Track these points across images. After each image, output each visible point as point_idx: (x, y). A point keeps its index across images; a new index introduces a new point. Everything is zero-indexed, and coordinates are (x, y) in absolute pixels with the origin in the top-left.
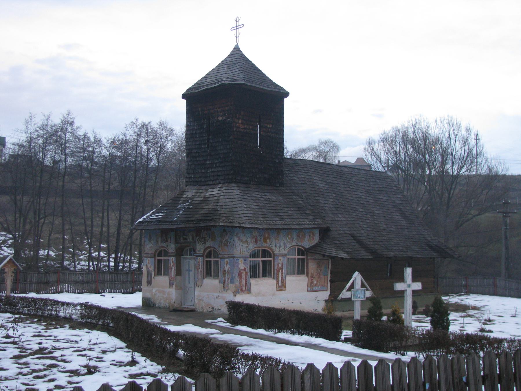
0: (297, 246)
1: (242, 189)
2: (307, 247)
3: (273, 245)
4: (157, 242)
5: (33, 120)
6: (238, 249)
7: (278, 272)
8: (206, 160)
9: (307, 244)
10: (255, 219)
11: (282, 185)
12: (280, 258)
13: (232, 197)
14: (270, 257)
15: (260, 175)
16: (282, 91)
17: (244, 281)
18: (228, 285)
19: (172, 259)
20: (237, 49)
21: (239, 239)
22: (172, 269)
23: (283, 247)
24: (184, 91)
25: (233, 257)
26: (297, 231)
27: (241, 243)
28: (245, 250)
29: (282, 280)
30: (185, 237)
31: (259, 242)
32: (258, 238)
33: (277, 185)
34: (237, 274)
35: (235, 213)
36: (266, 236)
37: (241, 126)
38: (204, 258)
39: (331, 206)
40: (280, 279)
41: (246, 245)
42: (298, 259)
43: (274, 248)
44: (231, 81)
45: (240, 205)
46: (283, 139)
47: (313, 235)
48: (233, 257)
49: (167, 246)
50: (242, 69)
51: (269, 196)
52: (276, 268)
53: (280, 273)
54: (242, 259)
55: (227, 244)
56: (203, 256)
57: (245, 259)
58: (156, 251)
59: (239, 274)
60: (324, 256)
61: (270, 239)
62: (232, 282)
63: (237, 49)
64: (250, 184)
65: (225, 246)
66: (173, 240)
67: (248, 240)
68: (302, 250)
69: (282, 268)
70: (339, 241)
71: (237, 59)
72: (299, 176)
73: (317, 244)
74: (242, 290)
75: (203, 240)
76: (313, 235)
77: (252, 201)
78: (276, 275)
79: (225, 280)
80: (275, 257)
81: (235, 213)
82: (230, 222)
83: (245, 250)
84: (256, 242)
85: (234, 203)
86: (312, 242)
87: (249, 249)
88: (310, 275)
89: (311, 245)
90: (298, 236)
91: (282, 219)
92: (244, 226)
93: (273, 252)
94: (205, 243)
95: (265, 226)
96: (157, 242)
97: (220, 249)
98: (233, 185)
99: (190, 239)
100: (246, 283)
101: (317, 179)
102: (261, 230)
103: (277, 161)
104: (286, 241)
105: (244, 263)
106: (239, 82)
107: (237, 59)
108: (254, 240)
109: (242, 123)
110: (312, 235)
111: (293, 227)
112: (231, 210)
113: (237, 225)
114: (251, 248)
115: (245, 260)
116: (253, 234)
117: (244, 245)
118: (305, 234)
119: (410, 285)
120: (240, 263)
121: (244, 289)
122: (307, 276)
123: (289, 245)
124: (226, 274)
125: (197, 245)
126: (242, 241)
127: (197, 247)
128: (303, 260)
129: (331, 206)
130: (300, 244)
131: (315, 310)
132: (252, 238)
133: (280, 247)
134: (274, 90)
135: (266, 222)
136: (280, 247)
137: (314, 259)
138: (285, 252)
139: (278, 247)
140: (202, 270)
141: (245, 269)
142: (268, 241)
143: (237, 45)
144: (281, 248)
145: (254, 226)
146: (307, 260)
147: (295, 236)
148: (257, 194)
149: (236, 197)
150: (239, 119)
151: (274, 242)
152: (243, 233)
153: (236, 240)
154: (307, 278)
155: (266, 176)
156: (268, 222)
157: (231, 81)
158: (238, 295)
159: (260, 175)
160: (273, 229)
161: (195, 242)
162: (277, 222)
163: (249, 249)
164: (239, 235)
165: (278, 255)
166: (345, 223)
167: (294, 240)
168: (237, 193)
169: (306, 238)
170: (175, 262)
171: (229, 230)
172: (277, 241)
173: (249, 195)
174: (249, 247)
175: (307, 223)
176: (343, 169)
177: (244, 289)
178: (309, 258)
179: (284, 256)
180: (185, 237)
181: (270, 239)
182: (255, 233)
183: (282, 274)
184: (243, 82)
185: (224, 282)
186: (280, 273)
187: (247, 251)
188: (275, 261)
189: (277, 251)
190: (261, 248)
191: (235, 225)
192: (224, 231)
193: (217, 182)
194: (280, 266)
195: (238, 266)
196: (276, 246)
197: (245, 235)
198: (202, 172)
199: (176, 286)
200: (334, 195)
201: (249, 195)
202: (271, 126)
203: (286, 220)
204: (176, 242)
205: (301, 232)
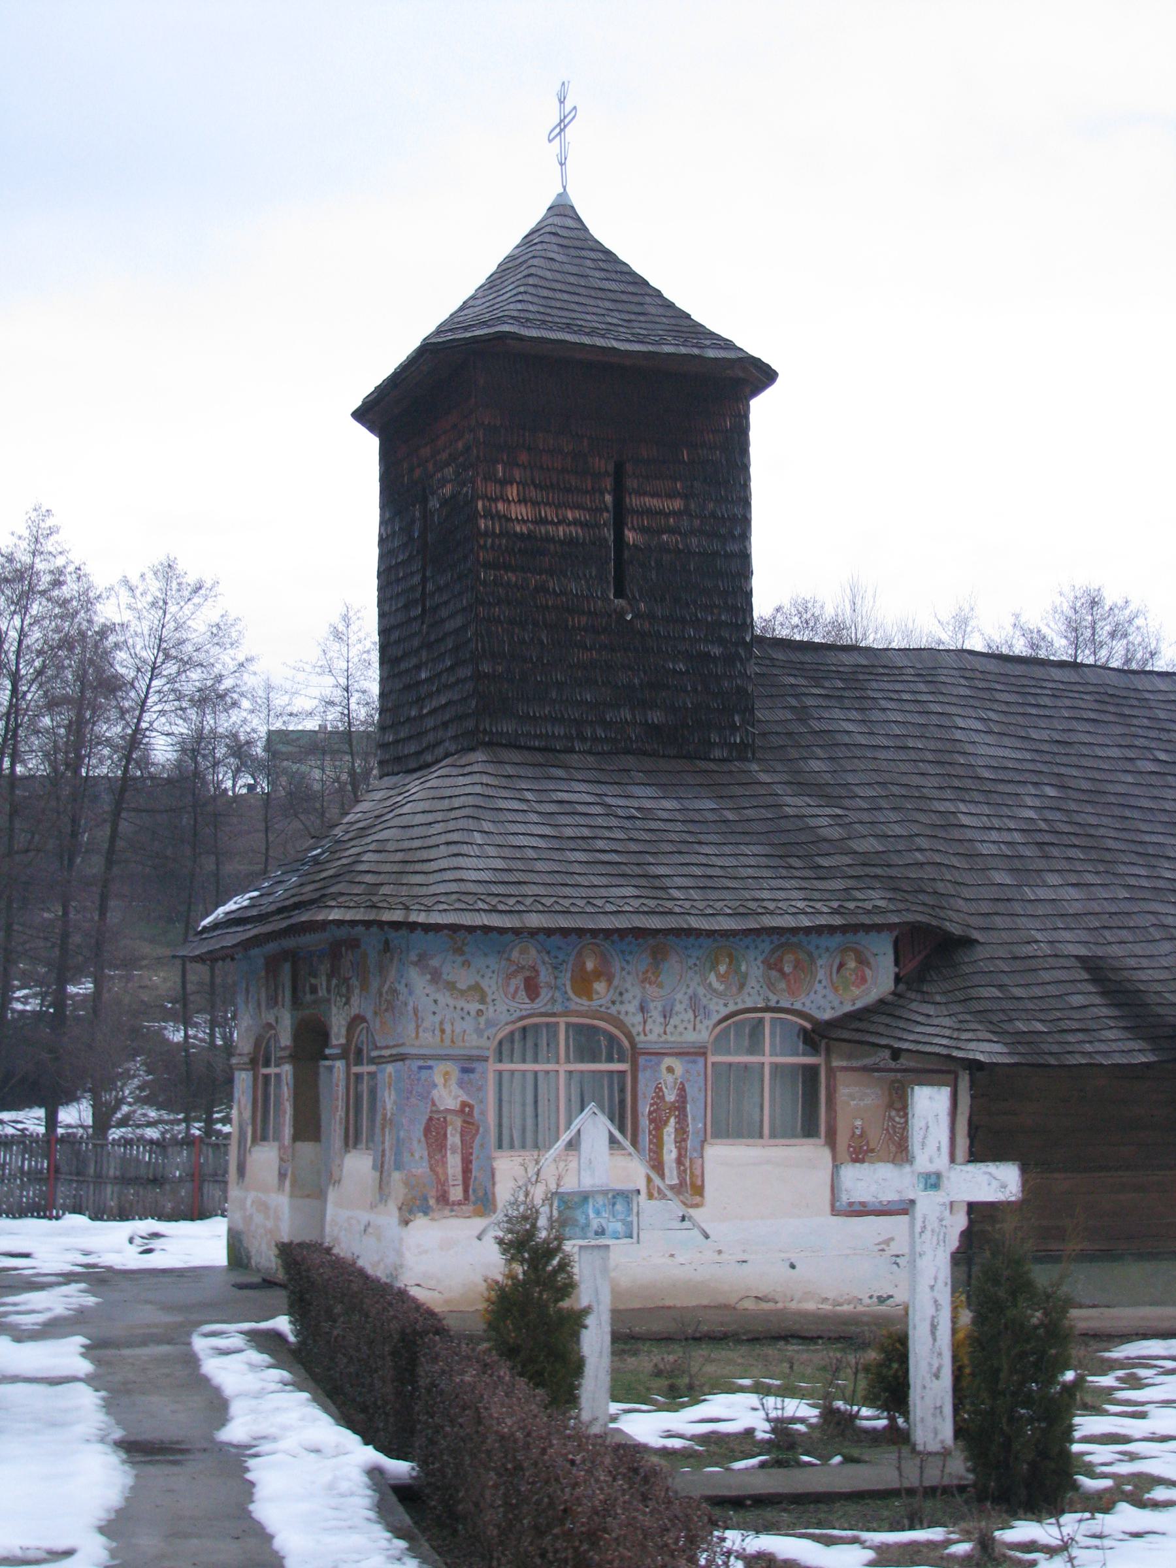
0: (767, 1009)
1: (510, 770)
2: (827, 1015)
3: (632, 1007)
4: (259, 1005)
5: (353, 628)
6: (429, 1021)
7: (658, 1124)
8: (418, 667)
9: (825, 1000)
10: (500, 889)
11: (744, 751)
12: (668, 1061)
13: (446, 804)
14: (621, 1060)
15: (626, 714)
16: (711, 354)
17: (454, 1163)
18: (389, 1175)
19: (287, 1069)
20: (562, 210)
21: (435, 976)
22: (285, 1112)
23: (683, 1014)
24: (358, 403)
25: (402, 1058)
26: (766, 946)
27: (445, 998)
28: (469, 1025)
29: (679, 1162)
30: (313, 981)
31: (545, 995)
32: (545, 976)
33: (717, 753)
34: (418, 1131)
35: (418, 867)
36: (590, 965)
37: (519, 511)
38: (348, 1066)
39: (1018, 837)
40: (670, 1154)
41: (474, 1007)
42: (775, 1067)
43: (634, 1020)
44: (465, 329)
45: (455, 837)
46: (745, 557)
47: (862, 961)
48: (402, 1058)
49: (277, 1019)
50: (531, 281)
51: (644, 796)
52: (645, 1109)
53: (669, 1132)
54: (453, 1068)
55: (389, 1004)
56: (344, 1056)
57: (468, 1065)
58: (257, 1045)
59: (427, 1131)
60: (896, 1054)
61: (610, 981)
62: (398, 1166)
63: (562, 210)
64: (571, 751)
65: (386, 1010)
66: (288, 994)
67: (484, 984)
68: (804, 1030)
69: (680, 1108)
70: (1000, 987)
71: (562, 248)
72: (876, 715)
73: (881, 1001)
74: (443, 1199)
75: (344, 990)
76: (862, 961)
77: (535, 818)
78: (645, 1139)
79: (383, 1151)
80: (642, 1060)
81: (418, 867)
82: (374, 906)
83: (469, 1025)
84: (532, 989)
85: (438, 828)
86: (856, 991)
87: (490, 1024)
88: (842, 1140)
89: (848, 1008)
90: (773, 965)
91: (656, 885)
92: (421, 918)
93: (629, 1036)
94: (347, 1003)
95: (534, 921)
96: (259, 1005)
97: (378, 1020)
98: (479, 756)
99: (322, 993)
100: (466, 1171)
101: (979, 726)
102: (556, 939)
103: (716, 651)
104: (701, 991)
105: (461, 1084)
106: (534, 333)
107: (562, 248)
108: (518, 981)
109: (522, 501)
110: (852, 964)
111: (695, 923)
112: (409, 856)
113: (397, 916)
114: (505, 1017)
115: (465, 1070)
116: (515, 955)
117: (461, 1003)
118: (813, 961)
119: (938, 1175)
120: (439, 1079)
121: (456, 1193)
122: (831, 1142)
123: (719, 1009)
124: (387, 1130)
125: (334, 1010)
126: (451, 986)
127: (334, 1020)
128: (810, 1073)
129: (1018, 837)
130: (784, 1004)
131: (882, 1300)
132: (509, 977)
133: (666, 1015)
134: (667, 349)
135: (548, 902)
136: (666, 1015)
137: (865, 1069)
138: (703, 1034)
139: (656, 1014)
140: (343, 1115)
141: (465, 1110)
142: (600, 986)
143: (563, 195)
144: (674, 1021)
145: (468, 919)
146: (831, 1072)
147: (753, 967)
148: (580, 793)
149: (457, 803)
150: (505, 482)
151: (634, 994)
152: (459, 951)
153: (418, 981)
154: (826, 1153)
155: (656, 717)
156: (567, 903)
157: (465, 329)
158: (420, 1222)
159: (626, 714)
160: (580, 932)
161: (329, 1001)
162: (622, 907)
163: (490, 1024)
164: (435, 963)
165: (656, 1048)
166: (1077, 907)
167: (752, 982)
168: (468, 790)
169: (821, 974)
170: (291, 1082)
171: (396, 938)
172: (651, 990)
173: (529, 796)
174: (490, 1013)
175: (790, 905)
176: (1140, 683)
177: (456, 1193)
178: (835, 1064)
179: (700, 1052)
180: (313, 981)
181: (610, 981)
182: (530, 955)
183: (681, 1131)
184: (506, 328)
185: (382, 1166)
186: (669, 1132)
187: (479, 1032)
188: (641, 1076)
189: (652, 1034)
190: (562, 1021)
191: (387, 916)
192: (387, 947)
193: (440, 751)
194: (671, 1097)
195: (426, 1096)
196: (642, 1009)
197: (467, 964)
198: (409, 719)
199: (293, 1185)
200: (1050, 791)
201: (529, 796)
202: (677, 504)
203: (675, 893)
204: (296, 1002)
205: (785, 945)
